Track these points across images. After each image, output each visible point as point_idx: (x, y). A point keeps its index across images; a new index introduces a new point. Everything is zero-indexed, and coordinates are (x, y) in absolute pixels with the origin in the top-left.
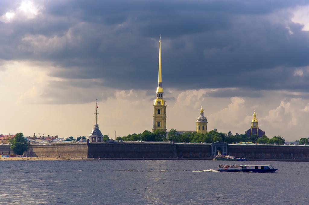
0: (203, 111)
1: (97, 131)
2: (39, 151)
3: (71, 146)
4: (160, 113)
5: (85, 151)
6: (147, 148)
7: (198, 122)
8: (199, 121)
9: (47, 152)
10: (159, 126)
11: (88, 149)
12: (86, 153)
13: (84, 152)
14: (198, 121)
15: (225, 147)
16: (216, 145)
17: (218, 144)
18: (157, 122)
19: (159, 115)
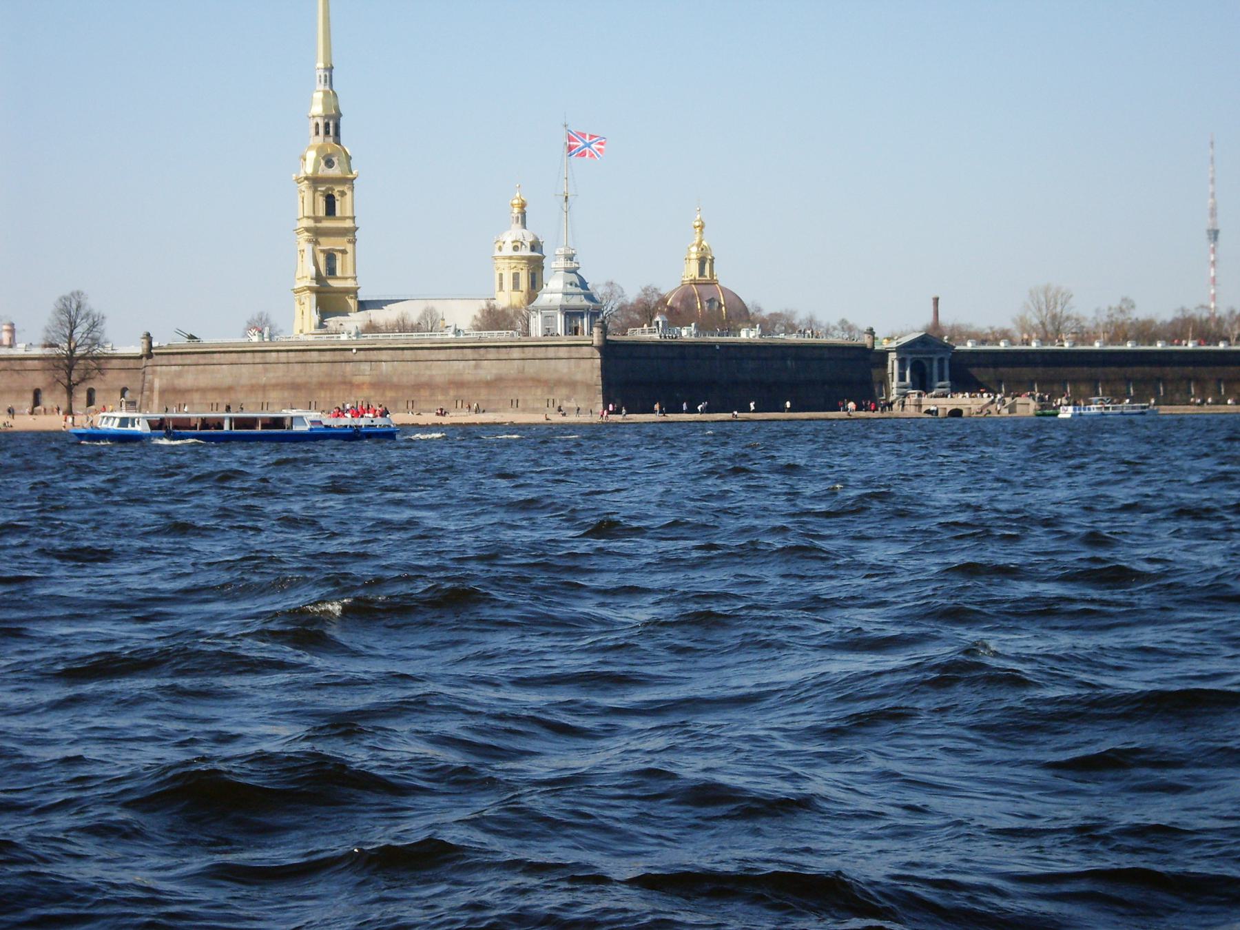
0: (523, 206)
1: (706, 282)
2: (228, 381)
3: (469, 353)
4: (338, 213)
5: (579, 377)
6: (789, 362)
7: (511, 258)
8: (516, 248)
9: (295, 387)
10: (331, 271)
11: (604, 369)
12: (588, 386)
13: (572, 385)
14: (508, 250)
15: (941, 361)
16: (911, 353)
17: (918, 347)
19: (328, 224)
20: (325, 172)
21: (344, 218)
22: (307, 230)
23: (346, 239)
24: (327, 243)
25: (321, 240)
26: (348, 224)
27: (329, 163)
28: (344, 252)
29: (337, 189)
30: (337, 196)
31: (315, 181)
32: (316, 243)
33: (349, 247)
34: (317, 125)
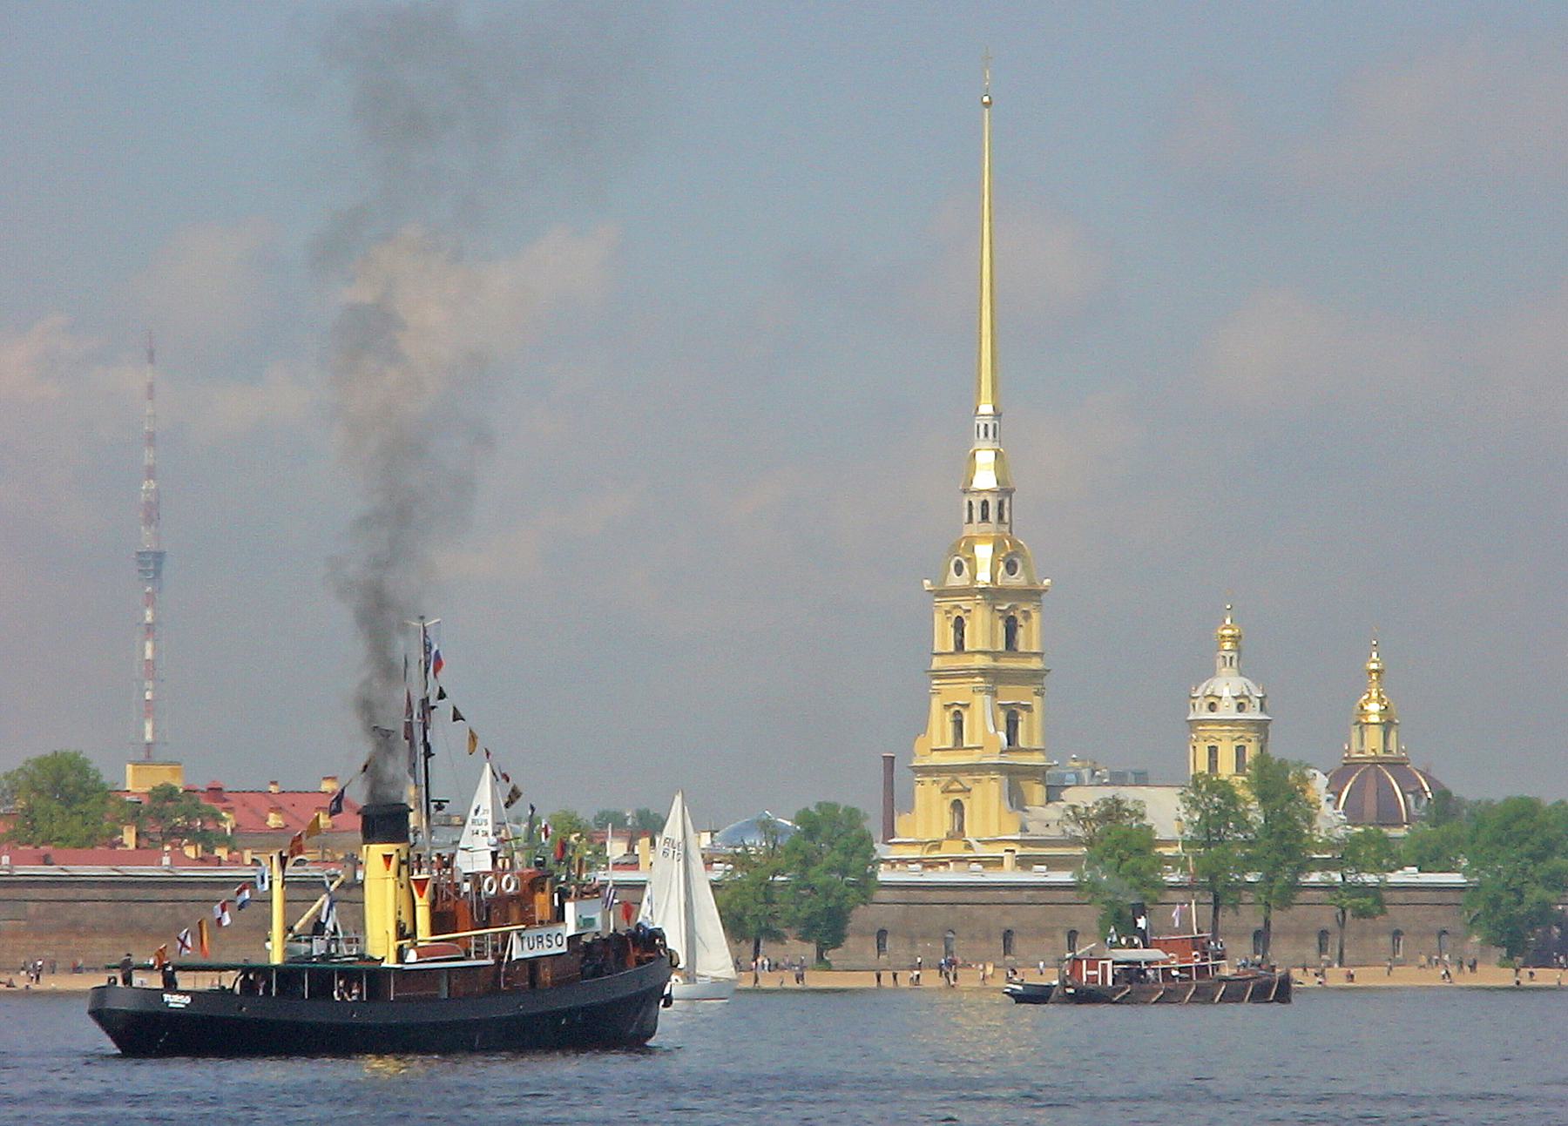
4: (1021, 647)
7: (1233, 722)
8: (1241, 707)
20: (1003, 580)
21: (1028, 655)
22: (983, 672)
23: (1033, 689)
24: (1012, 694)
25: (1000, 688)
26: (1035, 664)
27: (1011, 568)
28: (1028, 708)
30: (1021, 621)
31: (992, 594)
32: (995, 694)
33: (1037, 703)
34: (985, 504)
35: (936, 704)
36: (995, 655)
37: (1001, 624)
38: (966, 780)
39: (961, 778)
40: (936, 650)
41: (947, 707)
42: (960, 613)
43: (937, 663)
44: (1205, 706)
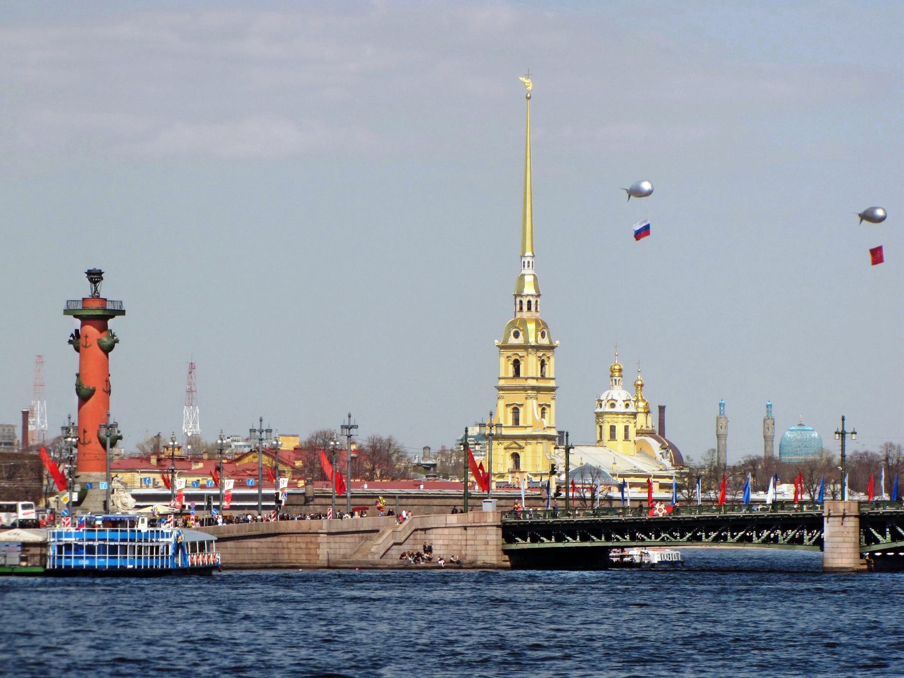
4: (547, 376)
7: (624, 414)
18: (540, 409)
25: (539, 396)
26: (552, 384)
28: (549, 406)
29: (549, 354)
34: (529, 302)
35: (501, 403)
36: (537, 379)
37: (539, 363)
38: (522, 443)
39: (518, 442)
40: (502, 375)
41: (507, 405)
42: (517, 358)
43: (502, 383)
44: (608, 405)
